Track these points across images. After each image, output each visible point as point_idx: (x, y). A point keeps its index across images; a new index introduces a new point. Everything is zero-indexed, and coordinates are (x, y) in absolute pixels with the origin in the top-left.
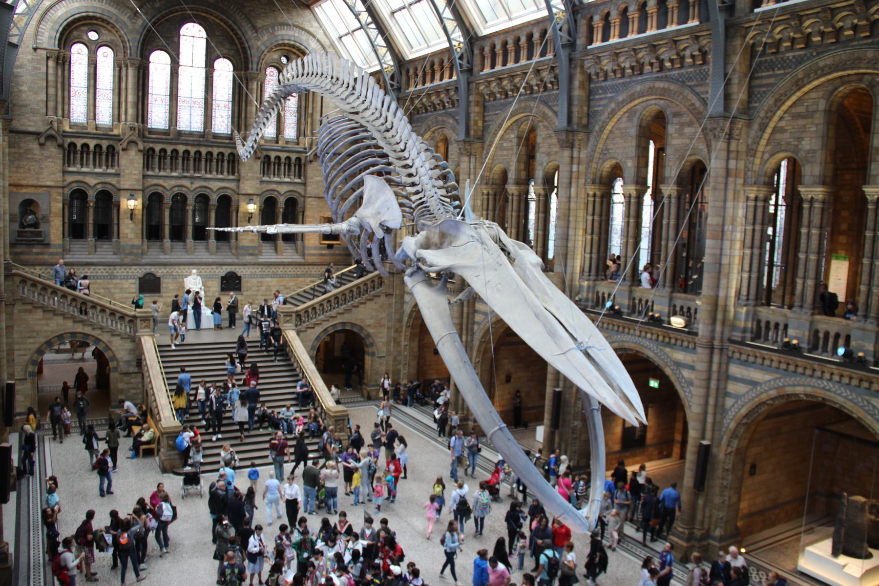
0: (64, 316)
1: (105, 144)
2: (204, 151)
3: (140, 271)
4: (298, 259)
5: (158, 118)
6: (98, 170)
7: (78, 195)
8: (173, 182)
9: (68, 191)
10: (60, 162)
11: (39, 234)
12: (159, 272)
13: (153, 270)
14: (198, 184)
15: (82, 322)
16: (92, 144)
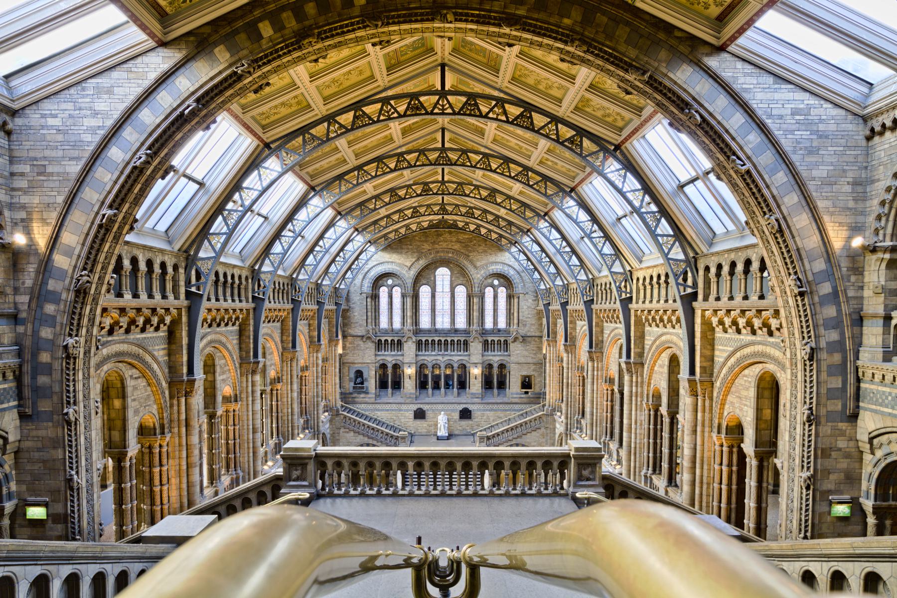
0: (363, 434)
1: (396, 339)
2: (449, 339)
3: (415, 407)
4: (506, 400)
5: (425, 322)
6: (393, 353)
7: (383, 366)
8: (433, 358)
9: (378, 365)
10: (373, 350)
11: (363, 388)
12: (425, 407)
13: (421, 406)
14: (446, 358)
15: (372, 438)
16: (389, 339)
